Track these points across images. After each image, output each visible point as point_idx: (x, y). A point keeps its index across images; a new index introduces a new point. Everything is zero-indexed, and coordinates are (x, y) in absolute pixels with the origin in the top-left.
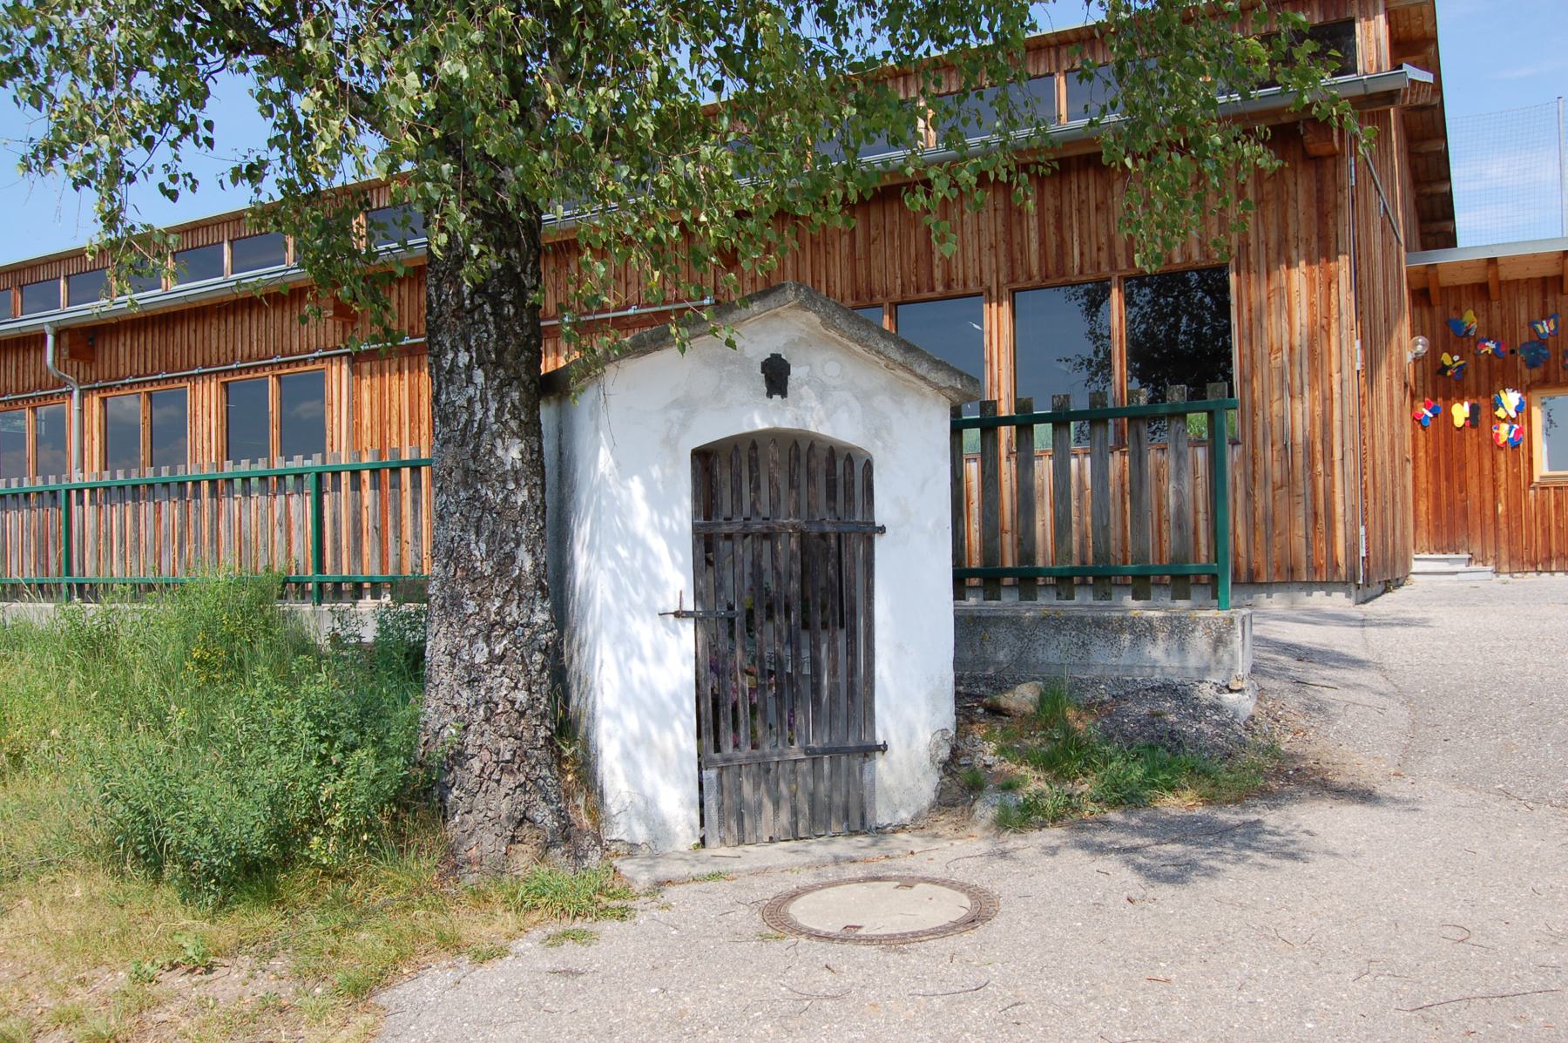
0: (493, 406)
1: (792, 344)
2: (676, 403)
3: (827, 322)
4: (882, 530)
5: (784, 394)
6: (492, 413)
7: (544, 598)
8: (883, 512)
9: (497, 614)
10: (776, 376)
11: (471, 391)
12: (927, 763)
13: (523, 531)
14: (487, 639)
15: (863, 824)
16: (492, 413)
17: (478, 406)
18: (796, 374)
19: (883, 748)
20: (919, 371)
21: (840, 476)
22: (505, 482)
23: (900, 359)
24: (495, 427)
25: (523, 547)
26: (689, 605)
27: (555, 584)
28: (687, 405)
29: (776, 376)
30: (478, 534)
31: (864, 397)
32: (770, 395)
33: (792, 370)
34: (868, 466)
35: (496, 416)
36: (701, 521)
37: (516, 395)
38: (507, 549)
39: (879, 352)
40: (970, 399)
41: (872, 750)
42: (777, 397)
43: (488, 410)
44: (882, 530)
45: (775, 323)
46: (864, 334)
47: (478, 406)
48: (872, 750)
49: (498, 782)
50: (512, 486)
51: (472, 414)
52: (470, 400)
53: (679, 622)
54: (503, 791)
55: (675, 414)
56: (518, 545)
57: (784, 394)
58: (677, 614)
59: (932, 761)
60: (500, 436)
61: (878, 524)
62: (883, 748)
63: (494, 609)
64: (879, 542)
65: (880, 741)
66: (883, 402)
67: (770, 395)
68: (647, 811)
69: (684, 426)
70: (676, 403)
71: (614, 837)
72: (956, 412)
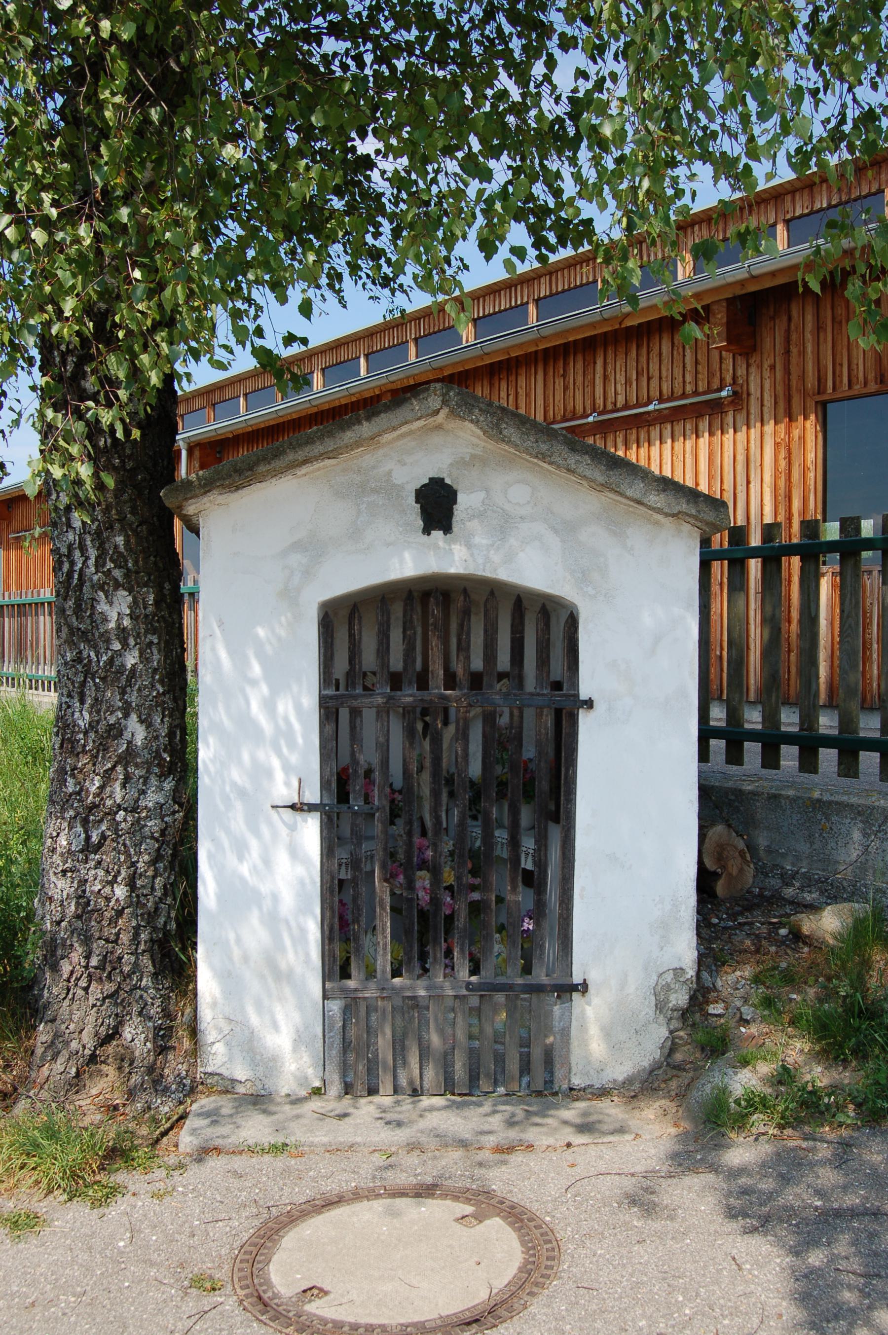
0: (93, 553)
1: (463, 464)
2: (297, 546)
3: (495, 432)
4: (589, 704)
5: (447, 529)
6: (91, 562)
7: (162, 777)
8: (588, 685)
9: (96, 795)
10: (437, 506)
11: (71, 536)
12: (648, 1009)
13: (133, 697)
14: (85, 822)
15: (549, 1083)
16: (91, 562)
17: (77, 554)
18: (465, 502)
19: (584, 988)
20: (629, 493)
21: (538, 635)
22: (108, 641)
23: (601, 479)
24: (95, 578)
25: (134, 717)
26: (313, 795)
27: (176, 759)
28: (313, 548)
29: (437, 506)
30: (82, 702)
31: (567, 530)
32: (427, 531)
33: (460, 497)
34: (572, 622)
35: (96, 566)
36: (331, 692)
37: (120, 540)
38: (112, 720)
39: (570, 471)
40: (718, 529)
41: (569, 989)
42: (437, 534)
43: (87, 558)
44: (589, 704)
45: (437, 439)
46: (544, 447)
47: (77, 554)
48: (569, 989)
49: (86, 989)
50: (117, 646)
51: (72, 563)
52: (70, 547)
53: (298, 817)
54: (92, 1001)
55: (296, 559)
56: (126, 716)
57: (447, 529)
58: (293, 807)
59: (660, 1006)
60: (102, 588)
61: (584, 695)
62: (584, 988)
63: (93, 789)
64: (586, 722)
65: (577, 979)
66: (594, 535)
67: (427, 531)
68: (249, 1046)
69: (308, 573)
70: (297, 546)
71: (209, 1070)
72: (705, 542)
